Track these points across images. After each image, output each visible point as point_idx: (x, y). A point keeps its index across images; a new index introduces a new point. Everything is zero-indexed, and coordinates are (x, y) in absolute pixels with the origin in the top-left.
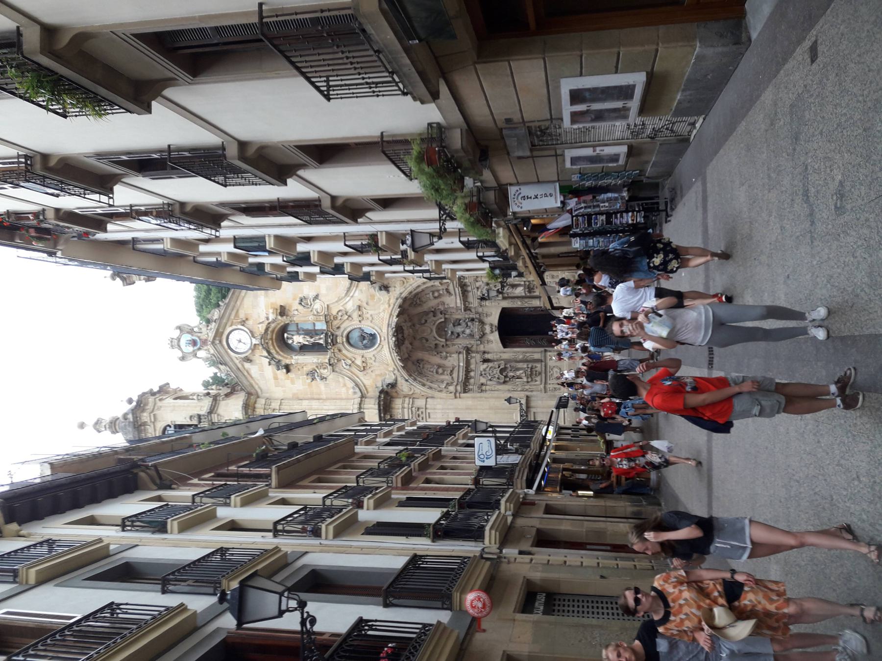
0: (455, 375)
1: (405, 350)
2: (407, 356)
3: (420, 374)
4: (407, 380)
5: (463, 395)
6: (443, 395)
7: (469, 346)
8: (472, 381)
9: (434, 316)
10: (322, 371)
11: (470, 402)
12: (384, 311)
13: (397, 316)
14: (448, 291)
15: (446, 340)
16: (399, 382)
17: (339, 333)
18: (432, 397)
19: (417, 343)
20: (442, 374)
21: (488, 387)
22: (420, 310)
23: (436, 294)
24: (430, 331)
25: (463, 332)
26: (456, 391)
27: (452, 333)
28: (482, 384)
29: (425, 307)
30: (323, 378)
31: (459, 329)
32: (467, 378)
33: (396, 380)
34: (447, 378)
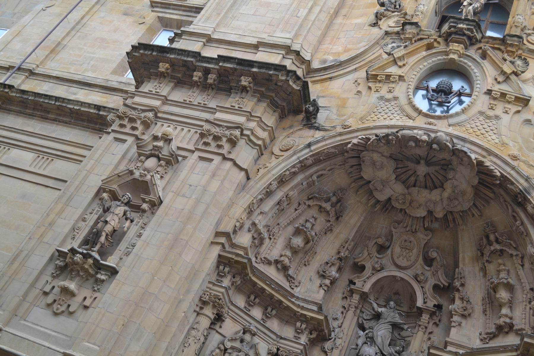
0: (271, 272)
1: (382, 174)
2: (367, 173)
3: (312, 196)
4: (309, 145)
5: (216, 251)
6: (238, 211)
7: (328, 345)
8: (240, 301)
9: (436, 287)
10: (396, 19)
11: (189, 257)
12: (504, 144)
13: (480, 163)
14: (502, 330)
15: (364, 297)
16: (311, 132)
17: (472, 52)
18: (242, 188)
19: (382, 225)
20: (289, 245)
21: (205, 323)
22: (467, 252)
23: (503, 295)
24: (402, 263)
25: (371, 340)
26: (233, 245)
27: (377, 316)
28: (219, 318)
29: (468, 268)
30: (378, 17)
31: (382, 332)
32: (257, 295)
33: (318, 129)
34: (275, 249)
